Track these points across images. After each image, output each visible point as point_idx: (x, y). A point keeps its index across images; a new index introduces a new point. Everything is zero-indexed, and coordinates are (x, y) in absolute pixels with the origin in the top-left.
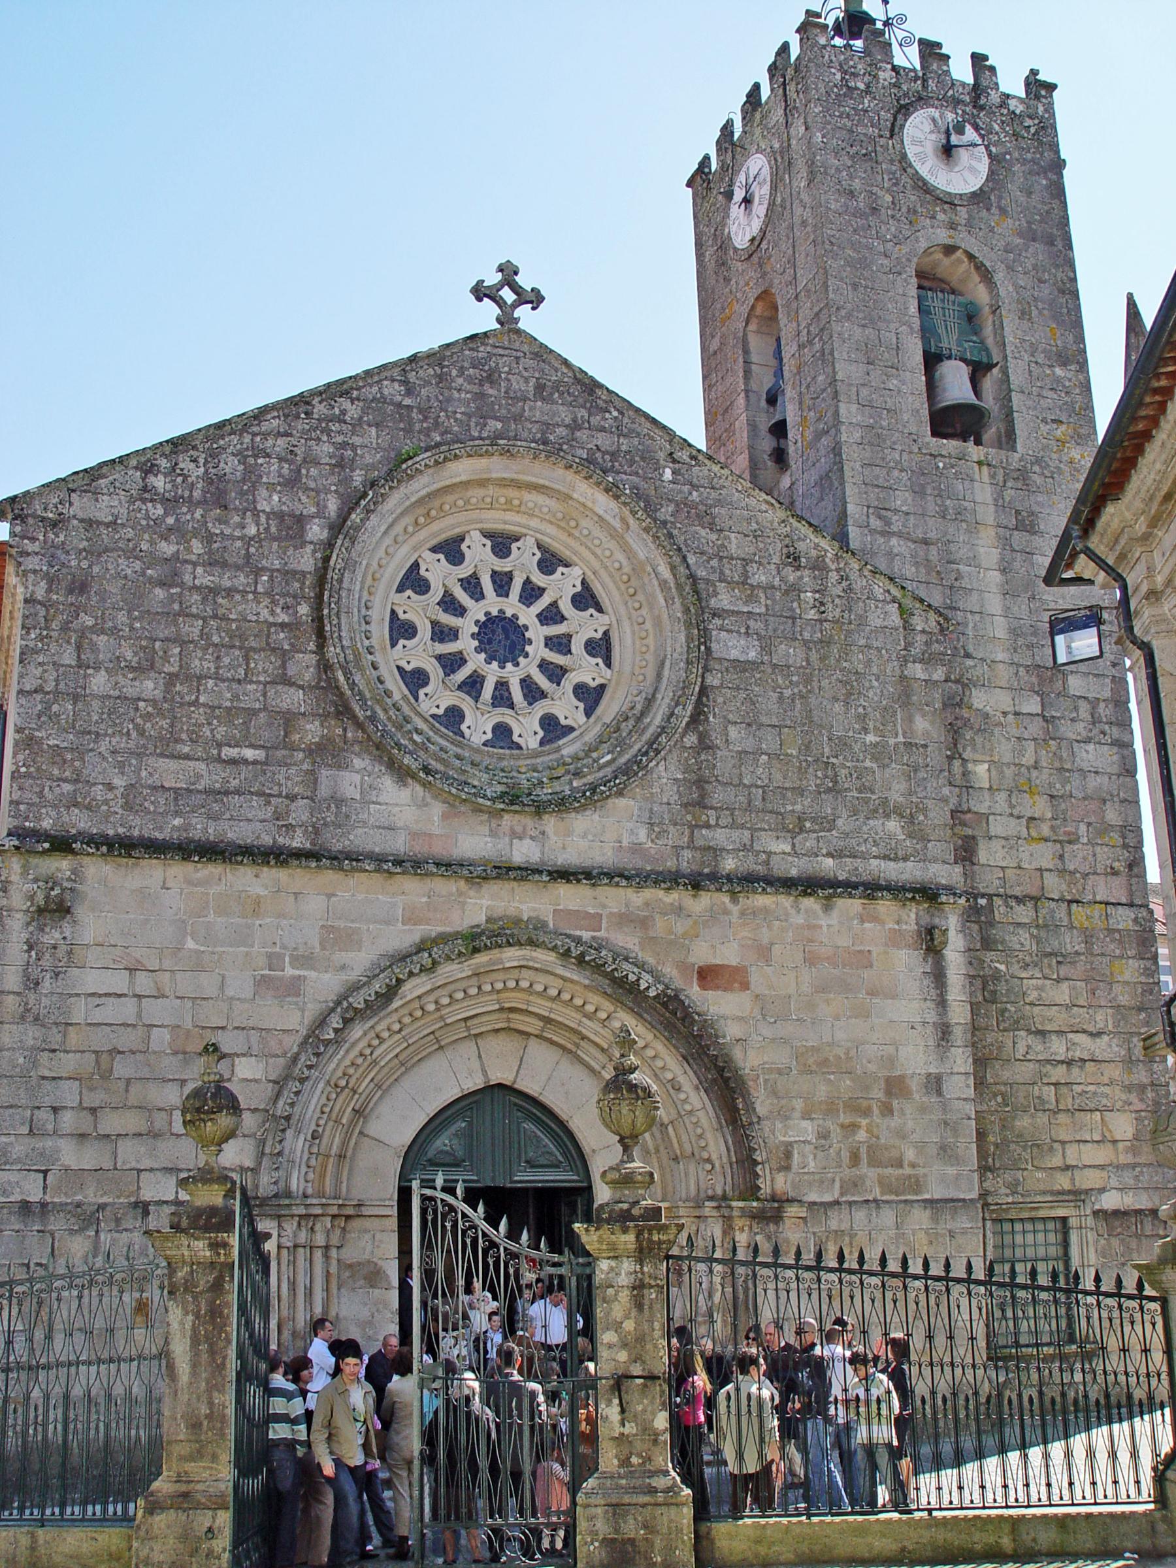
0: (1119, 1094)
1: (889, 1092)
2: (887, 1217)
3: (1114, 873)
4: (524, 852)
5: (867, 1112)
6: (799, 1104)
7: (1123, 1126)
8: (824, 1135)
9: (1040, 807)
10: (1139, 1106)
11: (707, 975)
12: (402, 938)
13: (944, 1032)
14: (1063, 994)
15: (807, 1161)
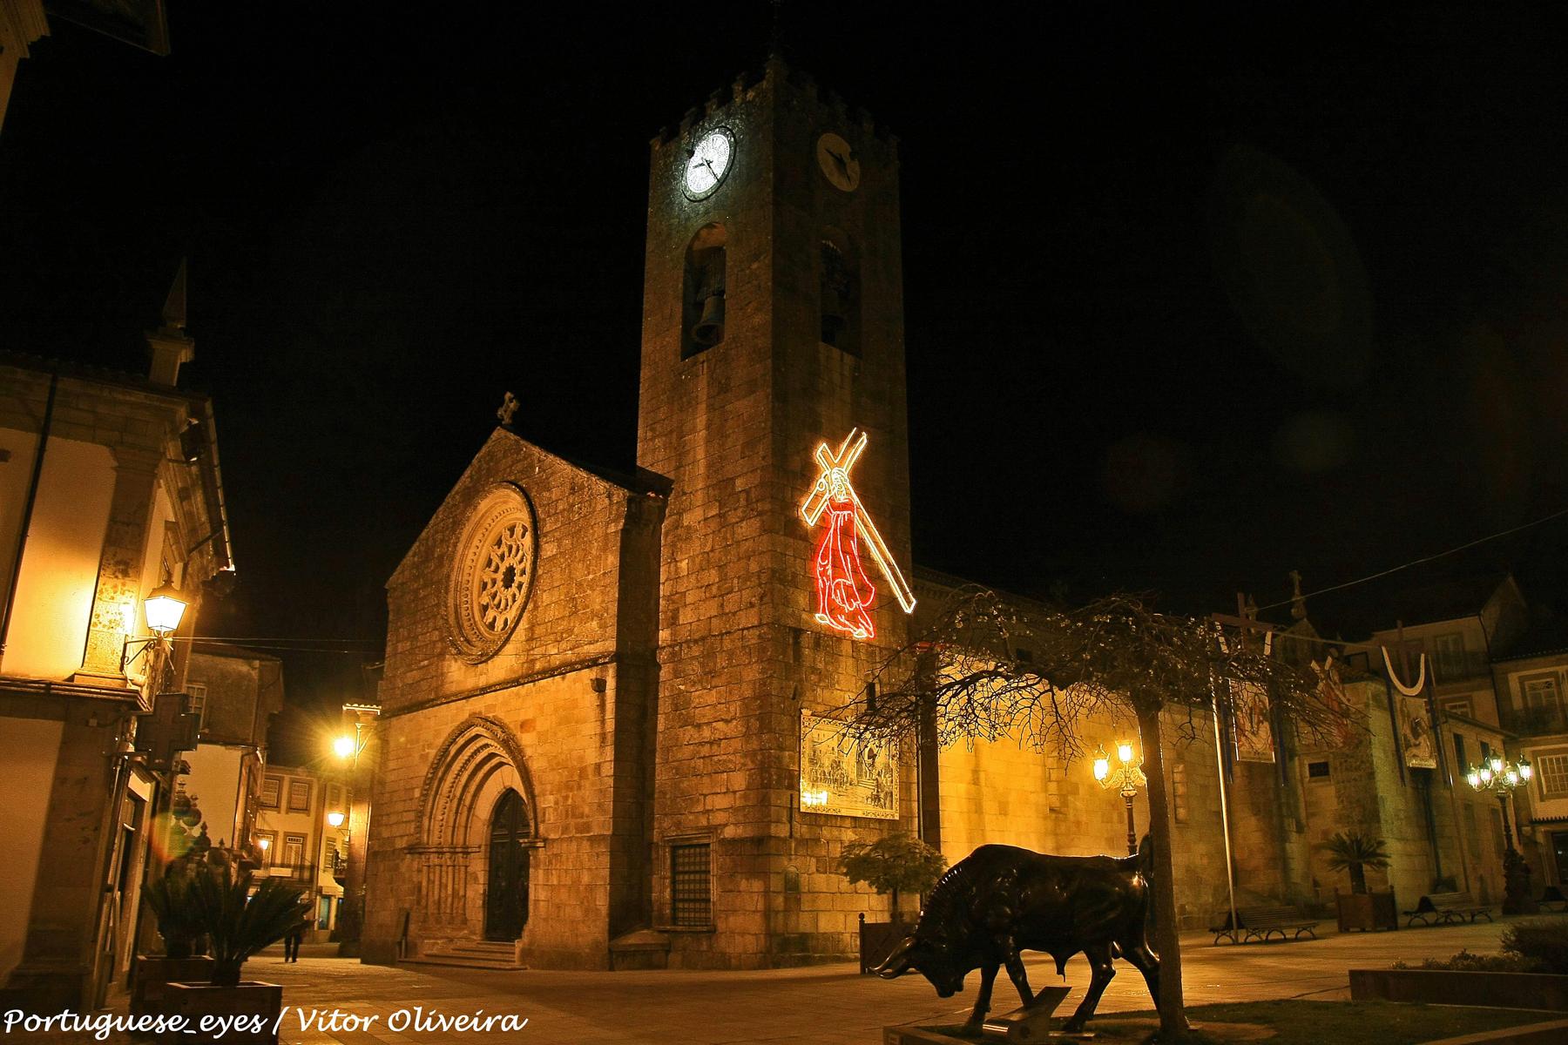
0: (738, 759)
1: (580, 776)
2: (574, 846)
3: (752, 605)
4: (482, 681)
5: (571, 789)
6: (549, 787)
7: (739, 781)
8: (556, 803)
9: (713, 576)
10: (751, 766)
11: (524, 725)
12: (447, 730)
13: (603, 736)
14: (712, 697)
15: (551, 817)
